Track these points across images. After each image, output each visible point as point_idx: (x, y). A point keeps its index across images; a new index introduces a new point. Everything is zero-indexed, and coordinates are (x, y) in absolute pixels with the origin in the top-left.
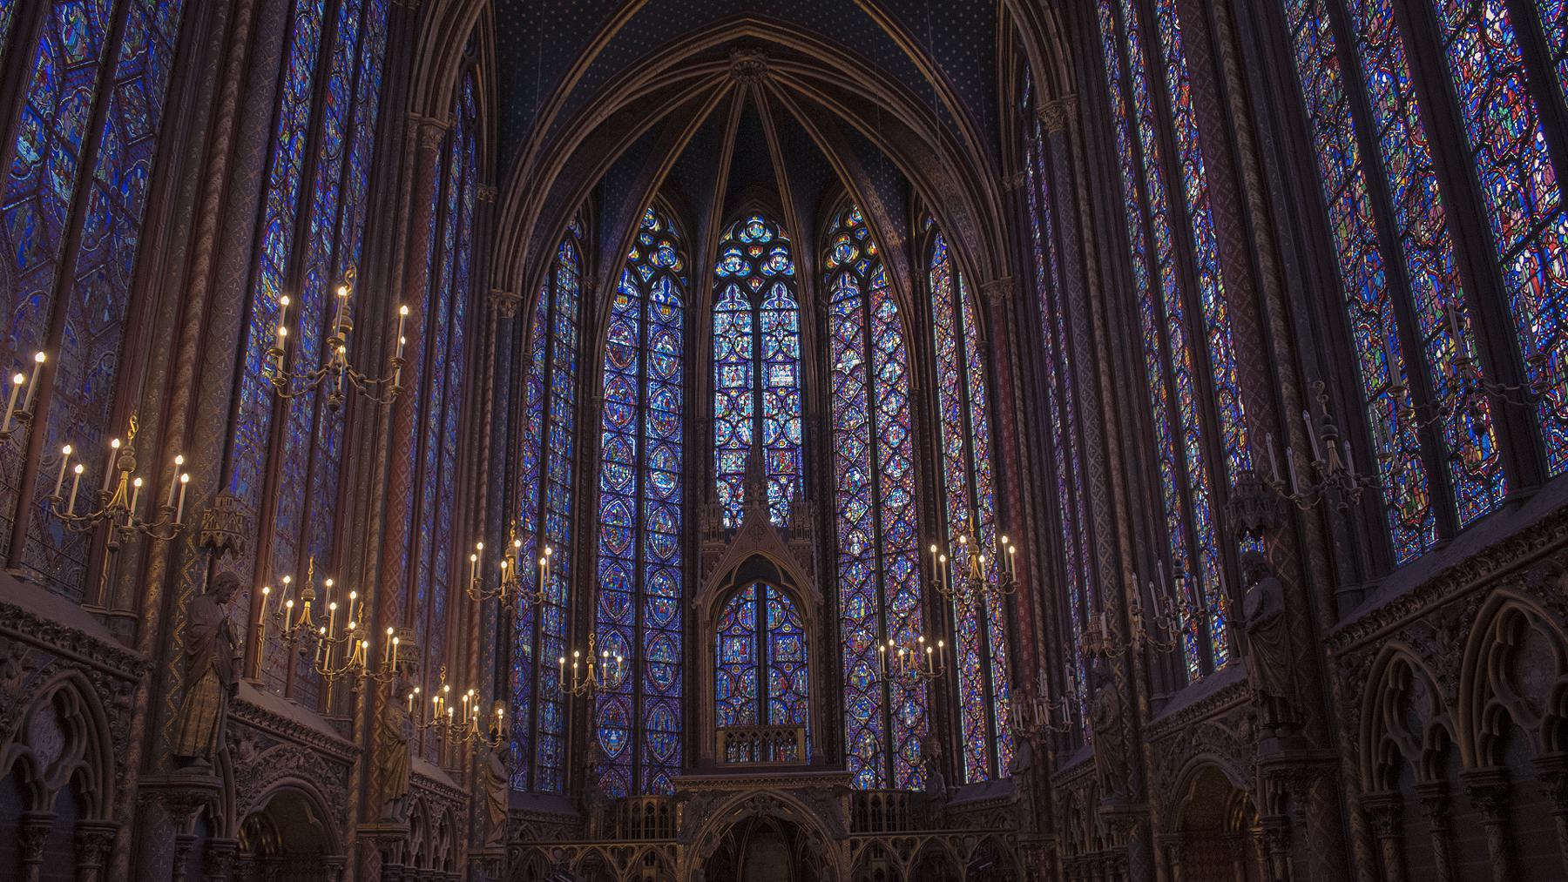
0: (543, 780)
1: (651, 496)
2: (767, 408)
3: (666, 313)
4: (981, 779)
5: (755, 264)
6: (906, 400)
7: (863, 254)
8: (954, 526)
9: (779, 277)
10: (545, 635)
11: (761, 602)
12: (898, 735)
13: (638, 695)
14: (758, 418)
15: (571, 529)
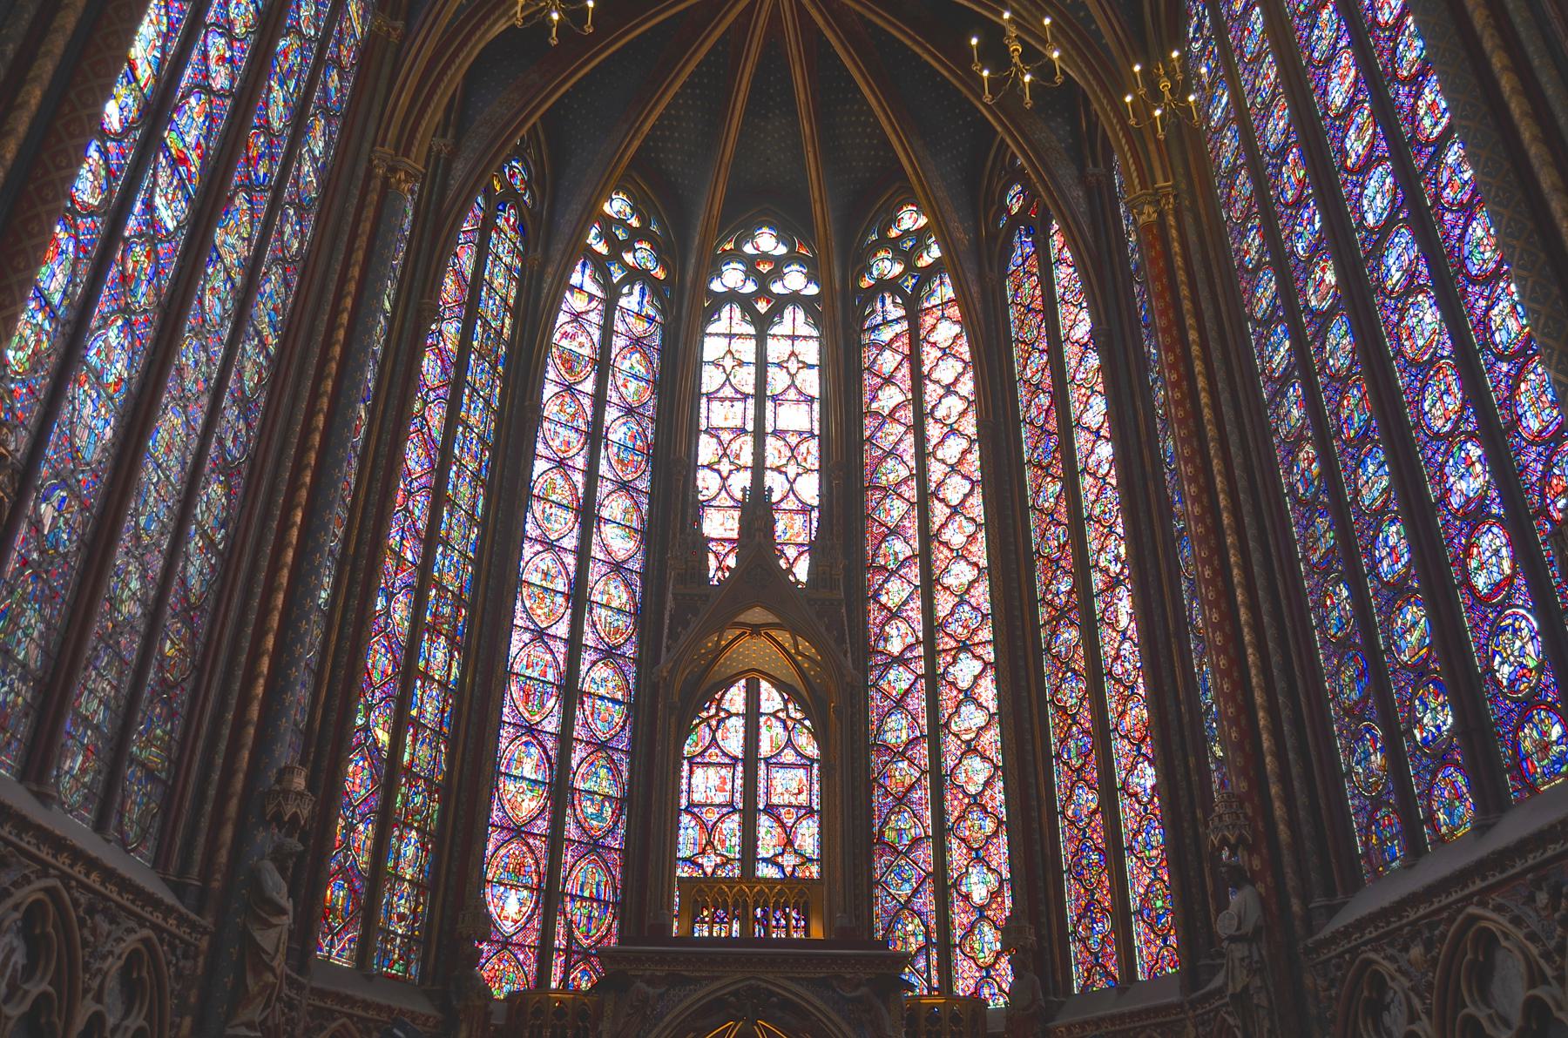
0: (386, 953)
1: (601, 556)
2: (771, 459)
3: (640, 327)
4: (1101, 984)
5: (763, 282)
6: (972, 442)
7: (910, 268)
8: (1050, 604)
9: (795, 298)
10: (416, 724)
11: (752, 715)
12: (960, 918)
13: (556, 840)
14: (758, 468)
15: (475, 578)
